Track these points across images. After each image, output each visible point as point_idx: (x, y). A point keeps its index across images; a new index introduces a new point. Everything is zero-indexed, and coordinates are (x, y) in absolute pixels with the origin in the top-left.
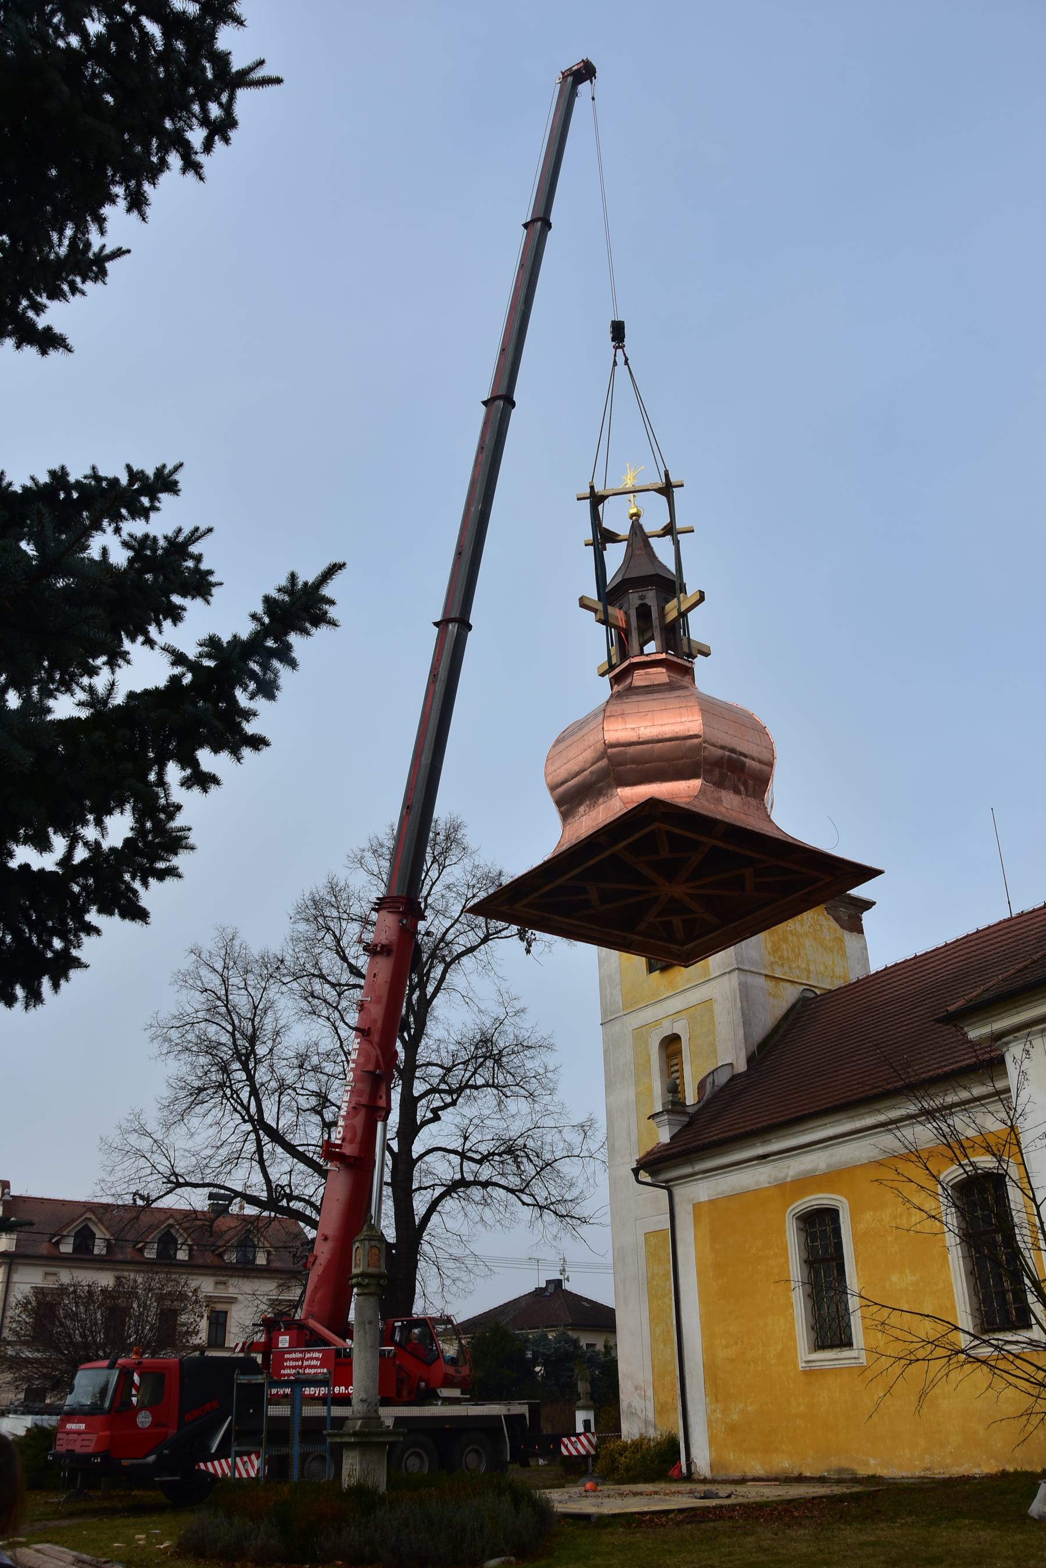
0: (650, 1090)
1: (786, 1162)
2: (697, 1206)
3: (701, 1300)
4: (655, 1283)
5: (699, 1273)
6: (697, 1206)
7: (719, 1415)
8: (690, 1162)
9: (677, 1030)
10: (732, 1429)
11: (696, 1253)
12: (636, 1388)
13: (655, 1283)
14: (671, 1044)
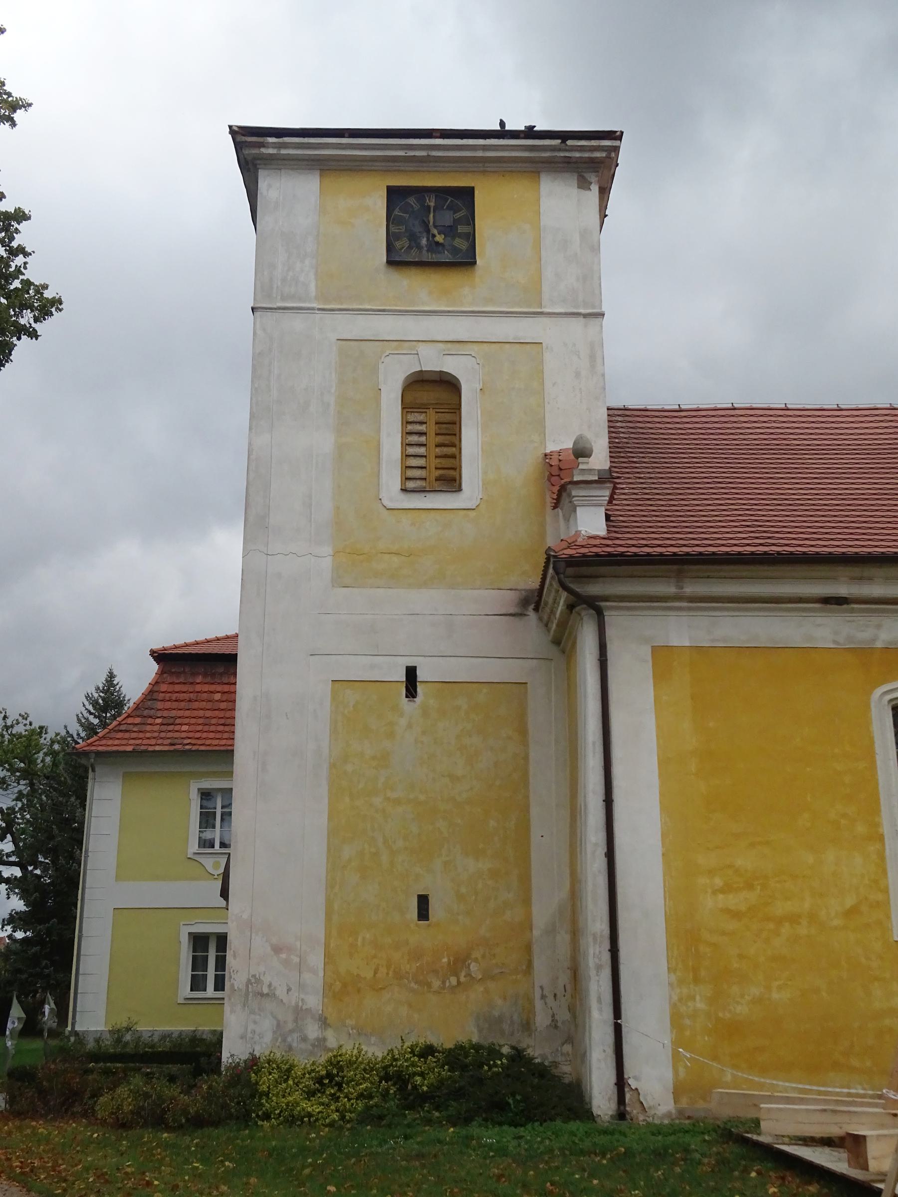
1: (875, 620)
3: (665, 809)
4: (349, 768)
5: (663, 763)
7: (700, 1005)
8: (680, 577)
9: (451, 366)
10: (730, 1030)
12: (277, 950)
13: (349, 768)
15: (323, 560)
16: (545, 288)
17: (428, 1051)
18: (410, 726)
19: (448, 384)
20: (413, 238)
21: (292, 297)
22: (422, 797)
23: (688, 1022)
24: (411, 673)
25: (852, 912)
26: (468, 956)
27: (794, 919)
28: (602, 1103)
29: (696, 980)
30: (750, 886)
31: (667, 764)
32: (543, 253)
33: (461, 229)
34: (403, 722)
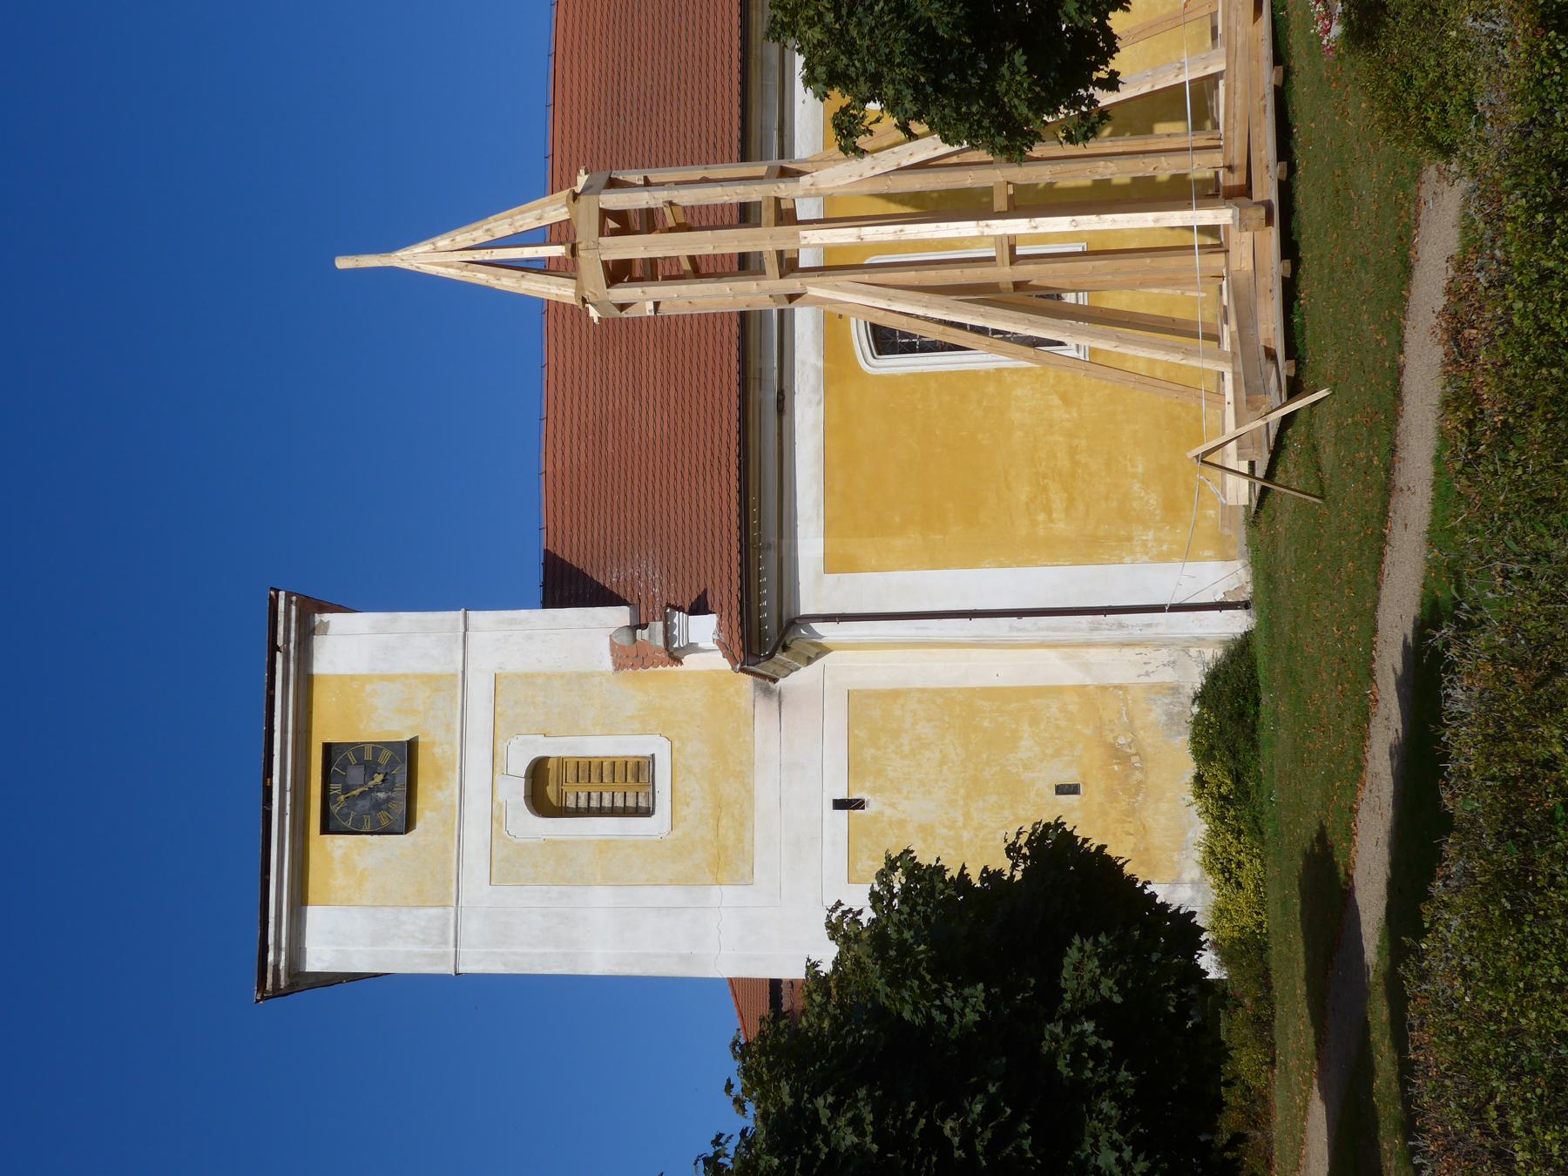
0: (605, 846)
2: (835, 563)
5: (934, 565)
6: (835, 563)
7: (1150, 535)
9: (520, 766)
10: (1172, 508)
11: (901, 569)
14: (544, 790)
15: (725, 894)
16: (436, 669)
17: (1199, 780)
18: (893, 805)
19: (538, 772)
20: (378, 806)
21: (444, 933)
22: (962, 791)
23: (1165, 547)
24: (840, 804)
25: (1064, 397)
26: (1112, 746)
27: (1073, 452)
28: (1237, 623)
29: (1129, 539)
30: (1045, 489)
31: (935, 561)
32: (398, 671)
33: (368, 756)
34: (888, 812)
